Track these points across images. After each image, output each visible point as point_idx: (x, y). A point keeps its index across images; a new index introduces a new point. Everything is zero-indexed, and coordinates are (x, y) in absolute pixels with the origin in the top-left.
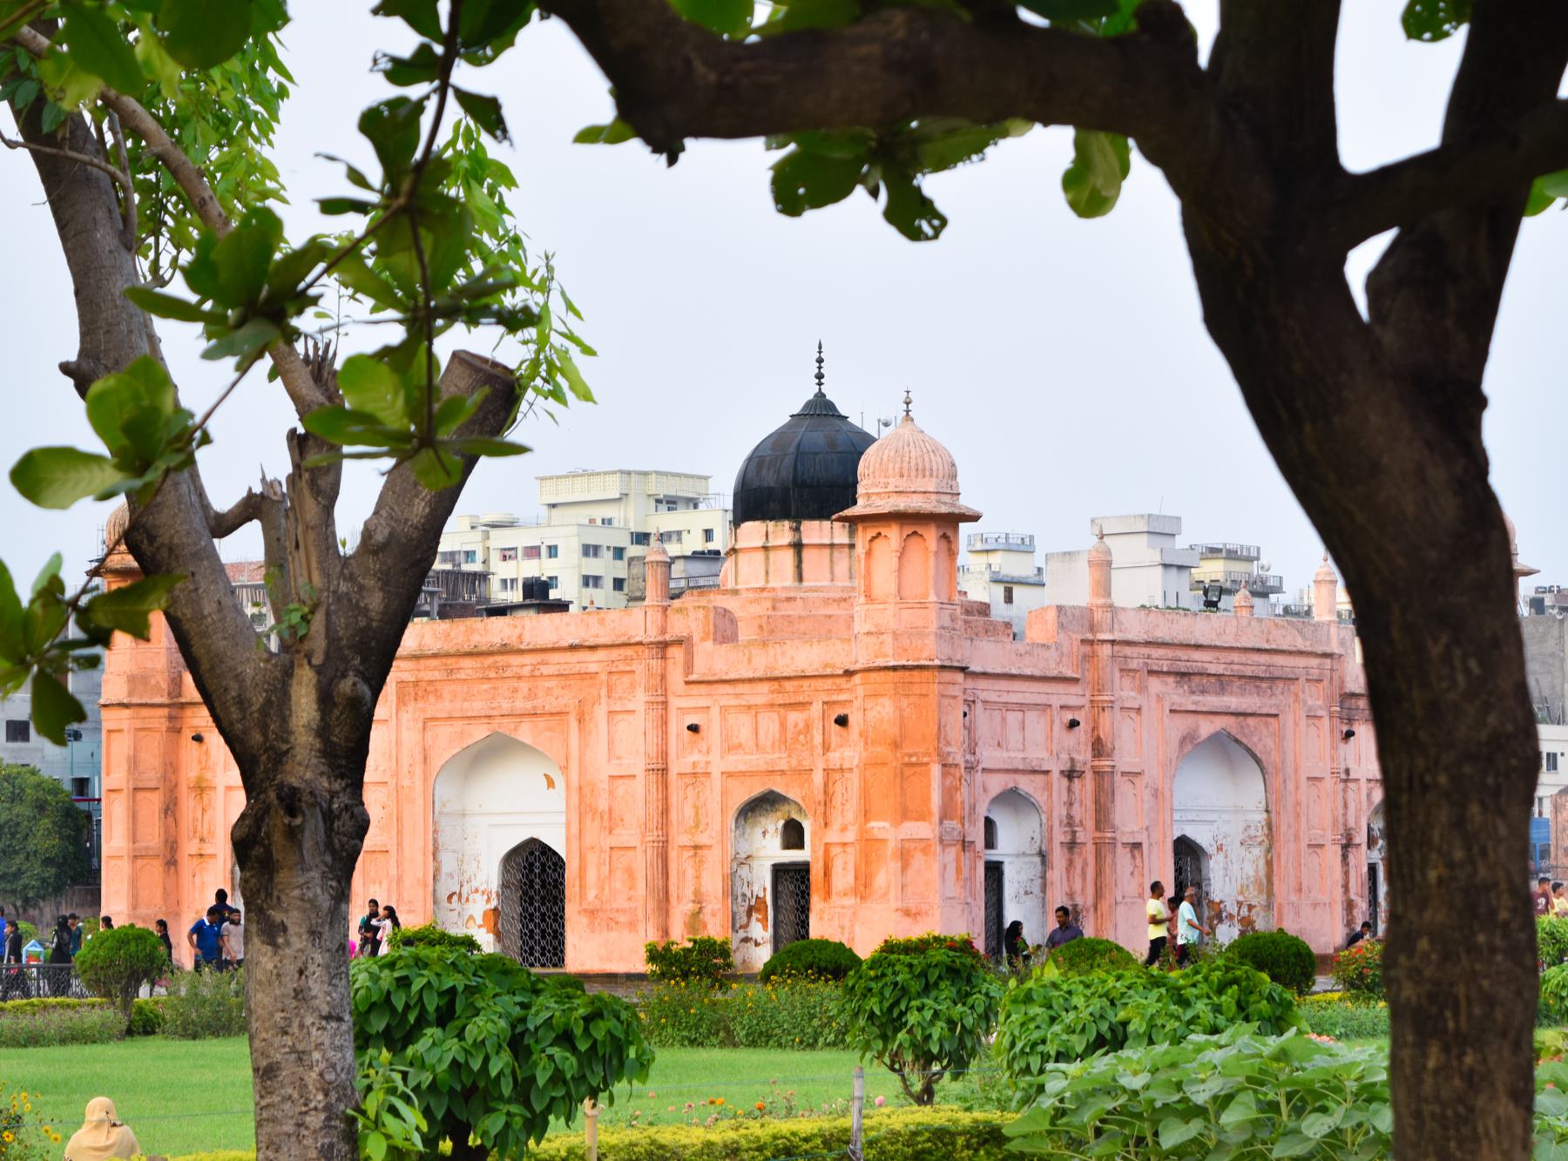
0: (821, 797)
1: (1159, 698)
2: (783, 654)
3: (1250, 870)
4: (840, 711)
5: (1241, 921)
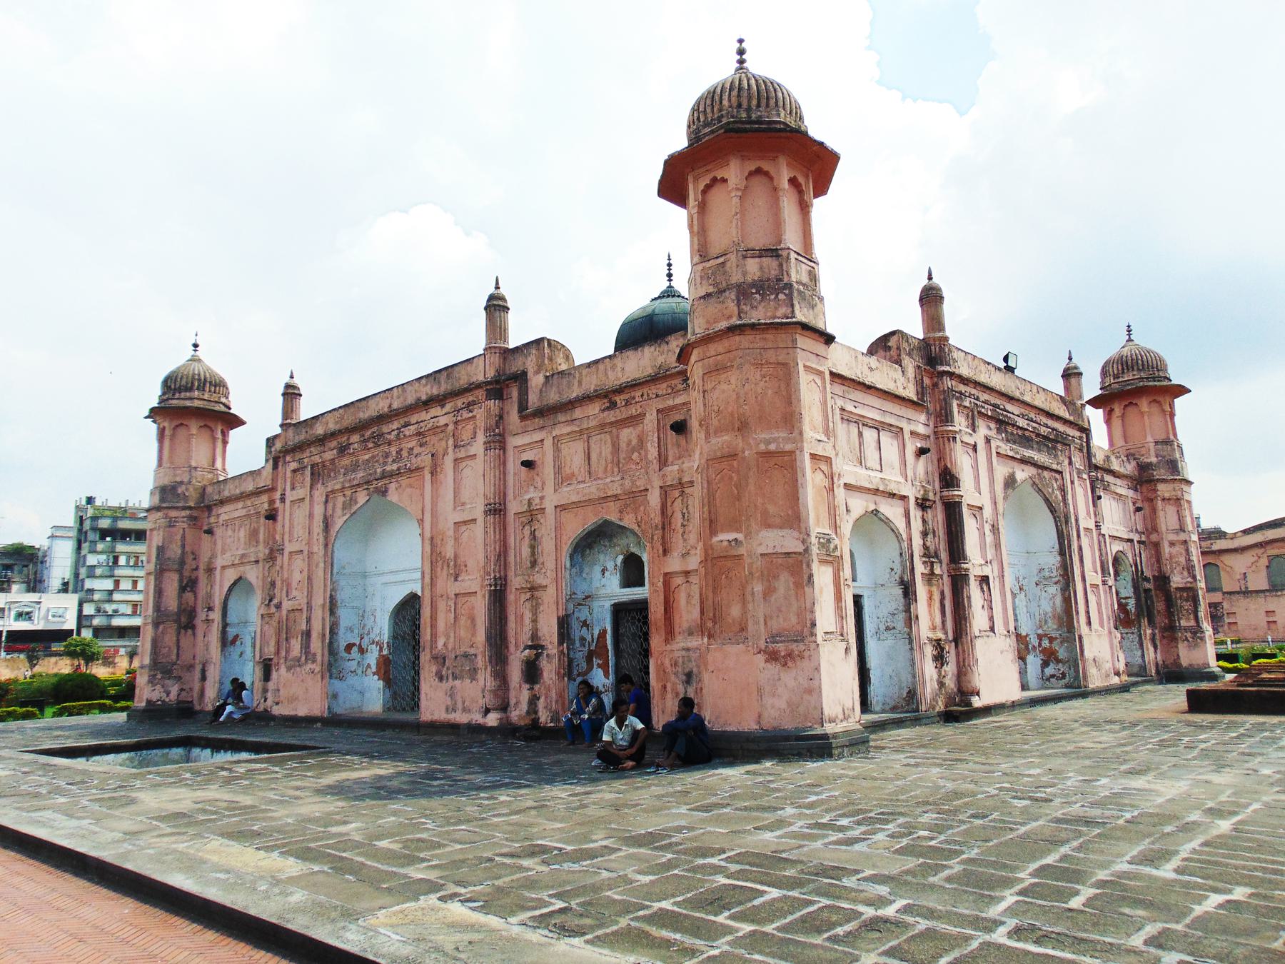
0: (658, 520)
1: (988, 440)
2: (613, 368)
3: (1047, 607)
4: (678, 417)
5: (1044, 651)
